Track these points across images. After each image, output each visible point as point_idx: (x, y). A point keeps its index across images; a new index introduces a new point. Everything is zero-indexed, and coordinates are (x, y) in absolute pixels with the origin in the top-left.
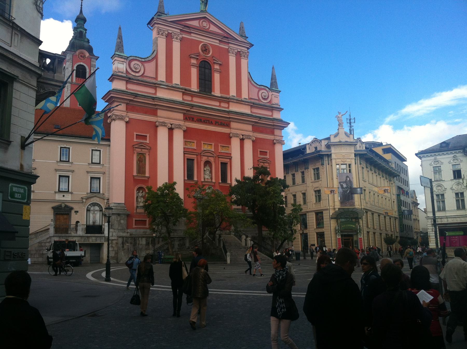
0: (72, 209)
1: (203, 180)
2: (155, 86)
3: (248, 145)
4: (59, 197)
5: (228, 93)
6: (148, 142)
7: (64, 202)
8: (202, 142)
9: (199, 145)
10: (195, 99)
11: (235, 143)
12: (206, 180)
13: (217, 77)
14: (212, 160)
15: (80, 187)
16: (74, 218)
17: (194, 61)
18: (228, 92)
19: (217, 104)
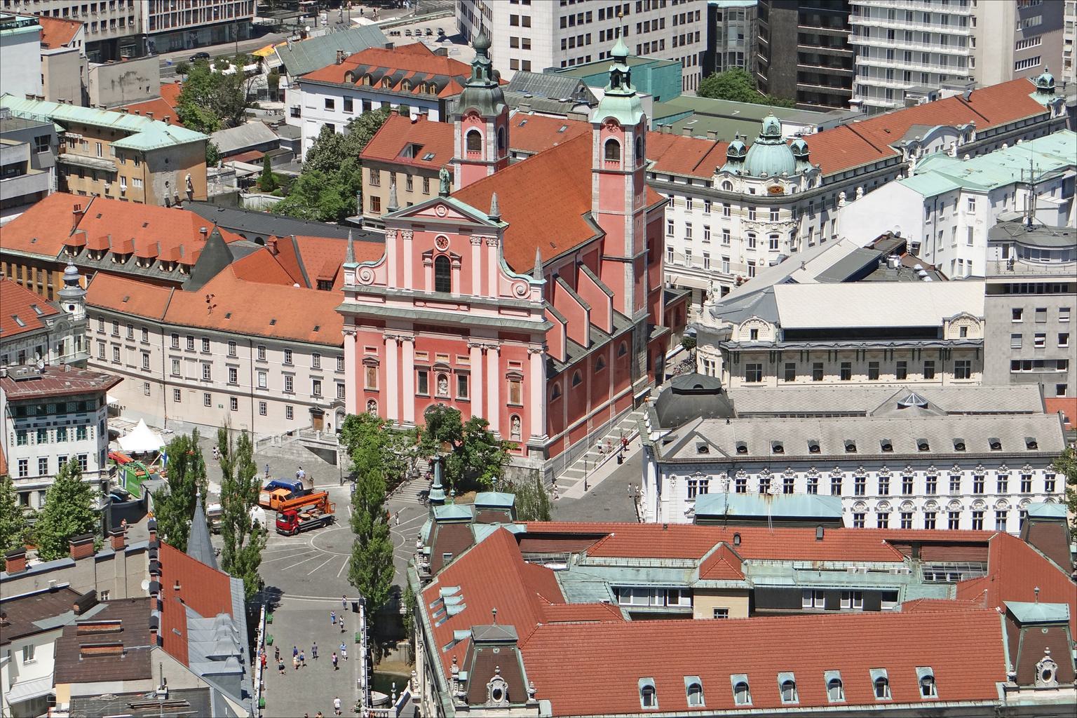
0: (323, 413)
1: (436, 395)
2: (385, 298)
3: (493, 356)
4: (313, 401)
5: (471, 293)
6: (376, 354)
7: (319, 405)
8: (436, 353)
9: (432, 357)
10: (428, 304)
11: (476, 354)
12: (440, 395)
13: (456, 274)
14: (447, 374)
15: (329, 393)
16: (326, 420)
17: (428, 260)
18: (470, 290)
19: (455, 307)
